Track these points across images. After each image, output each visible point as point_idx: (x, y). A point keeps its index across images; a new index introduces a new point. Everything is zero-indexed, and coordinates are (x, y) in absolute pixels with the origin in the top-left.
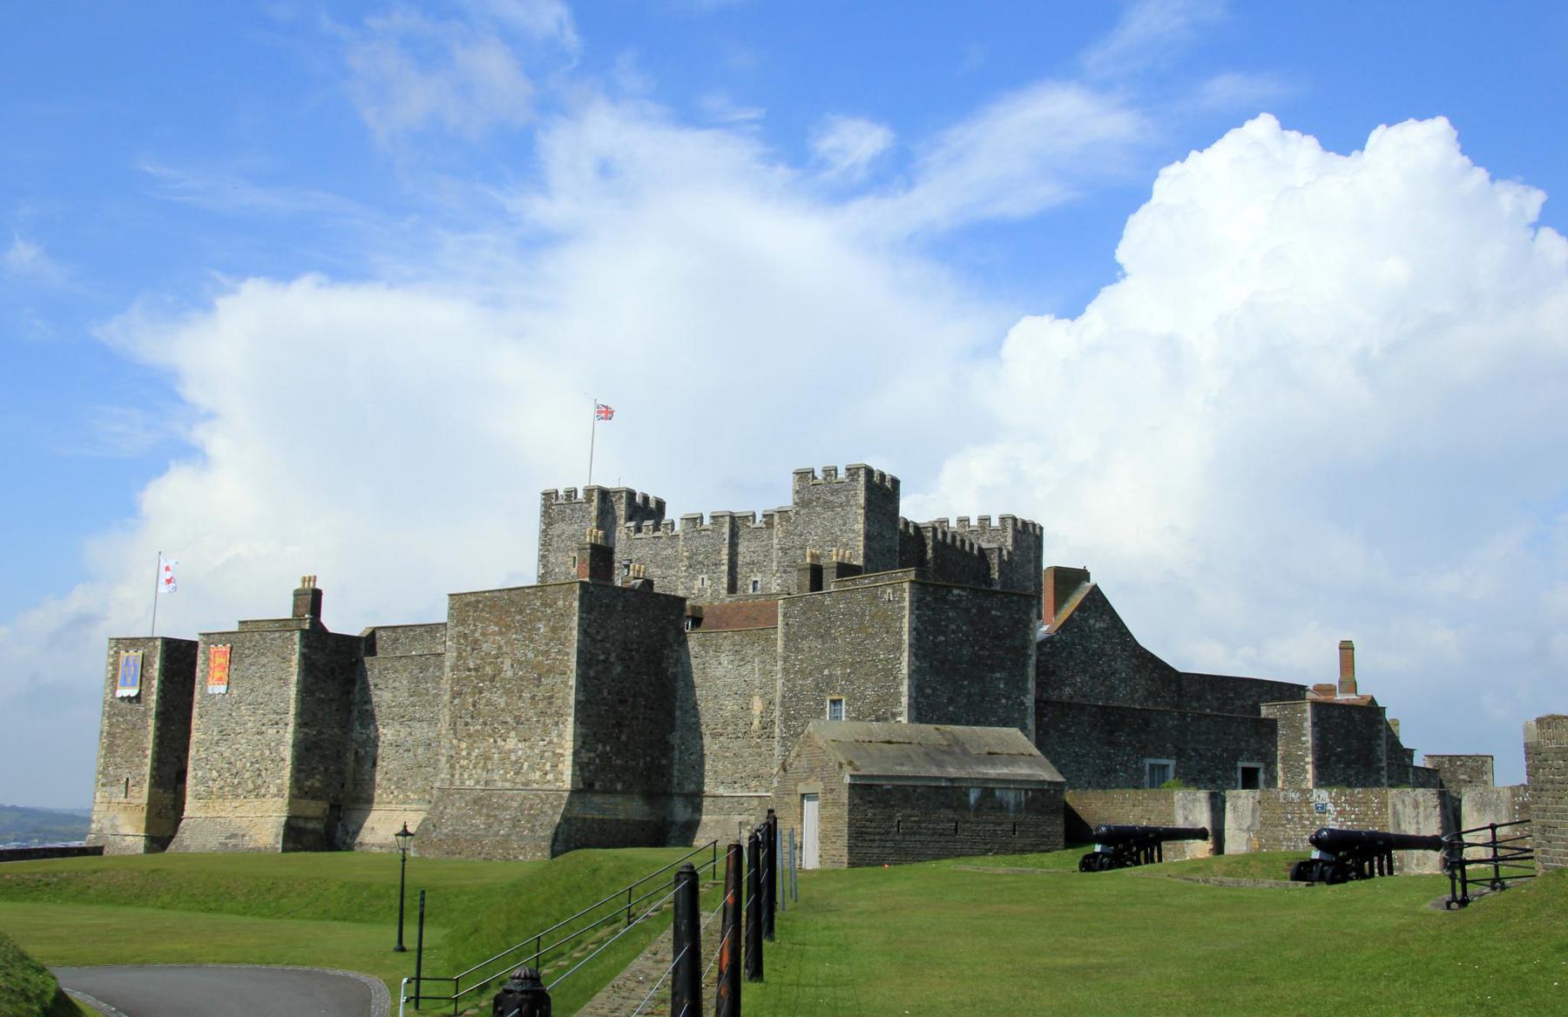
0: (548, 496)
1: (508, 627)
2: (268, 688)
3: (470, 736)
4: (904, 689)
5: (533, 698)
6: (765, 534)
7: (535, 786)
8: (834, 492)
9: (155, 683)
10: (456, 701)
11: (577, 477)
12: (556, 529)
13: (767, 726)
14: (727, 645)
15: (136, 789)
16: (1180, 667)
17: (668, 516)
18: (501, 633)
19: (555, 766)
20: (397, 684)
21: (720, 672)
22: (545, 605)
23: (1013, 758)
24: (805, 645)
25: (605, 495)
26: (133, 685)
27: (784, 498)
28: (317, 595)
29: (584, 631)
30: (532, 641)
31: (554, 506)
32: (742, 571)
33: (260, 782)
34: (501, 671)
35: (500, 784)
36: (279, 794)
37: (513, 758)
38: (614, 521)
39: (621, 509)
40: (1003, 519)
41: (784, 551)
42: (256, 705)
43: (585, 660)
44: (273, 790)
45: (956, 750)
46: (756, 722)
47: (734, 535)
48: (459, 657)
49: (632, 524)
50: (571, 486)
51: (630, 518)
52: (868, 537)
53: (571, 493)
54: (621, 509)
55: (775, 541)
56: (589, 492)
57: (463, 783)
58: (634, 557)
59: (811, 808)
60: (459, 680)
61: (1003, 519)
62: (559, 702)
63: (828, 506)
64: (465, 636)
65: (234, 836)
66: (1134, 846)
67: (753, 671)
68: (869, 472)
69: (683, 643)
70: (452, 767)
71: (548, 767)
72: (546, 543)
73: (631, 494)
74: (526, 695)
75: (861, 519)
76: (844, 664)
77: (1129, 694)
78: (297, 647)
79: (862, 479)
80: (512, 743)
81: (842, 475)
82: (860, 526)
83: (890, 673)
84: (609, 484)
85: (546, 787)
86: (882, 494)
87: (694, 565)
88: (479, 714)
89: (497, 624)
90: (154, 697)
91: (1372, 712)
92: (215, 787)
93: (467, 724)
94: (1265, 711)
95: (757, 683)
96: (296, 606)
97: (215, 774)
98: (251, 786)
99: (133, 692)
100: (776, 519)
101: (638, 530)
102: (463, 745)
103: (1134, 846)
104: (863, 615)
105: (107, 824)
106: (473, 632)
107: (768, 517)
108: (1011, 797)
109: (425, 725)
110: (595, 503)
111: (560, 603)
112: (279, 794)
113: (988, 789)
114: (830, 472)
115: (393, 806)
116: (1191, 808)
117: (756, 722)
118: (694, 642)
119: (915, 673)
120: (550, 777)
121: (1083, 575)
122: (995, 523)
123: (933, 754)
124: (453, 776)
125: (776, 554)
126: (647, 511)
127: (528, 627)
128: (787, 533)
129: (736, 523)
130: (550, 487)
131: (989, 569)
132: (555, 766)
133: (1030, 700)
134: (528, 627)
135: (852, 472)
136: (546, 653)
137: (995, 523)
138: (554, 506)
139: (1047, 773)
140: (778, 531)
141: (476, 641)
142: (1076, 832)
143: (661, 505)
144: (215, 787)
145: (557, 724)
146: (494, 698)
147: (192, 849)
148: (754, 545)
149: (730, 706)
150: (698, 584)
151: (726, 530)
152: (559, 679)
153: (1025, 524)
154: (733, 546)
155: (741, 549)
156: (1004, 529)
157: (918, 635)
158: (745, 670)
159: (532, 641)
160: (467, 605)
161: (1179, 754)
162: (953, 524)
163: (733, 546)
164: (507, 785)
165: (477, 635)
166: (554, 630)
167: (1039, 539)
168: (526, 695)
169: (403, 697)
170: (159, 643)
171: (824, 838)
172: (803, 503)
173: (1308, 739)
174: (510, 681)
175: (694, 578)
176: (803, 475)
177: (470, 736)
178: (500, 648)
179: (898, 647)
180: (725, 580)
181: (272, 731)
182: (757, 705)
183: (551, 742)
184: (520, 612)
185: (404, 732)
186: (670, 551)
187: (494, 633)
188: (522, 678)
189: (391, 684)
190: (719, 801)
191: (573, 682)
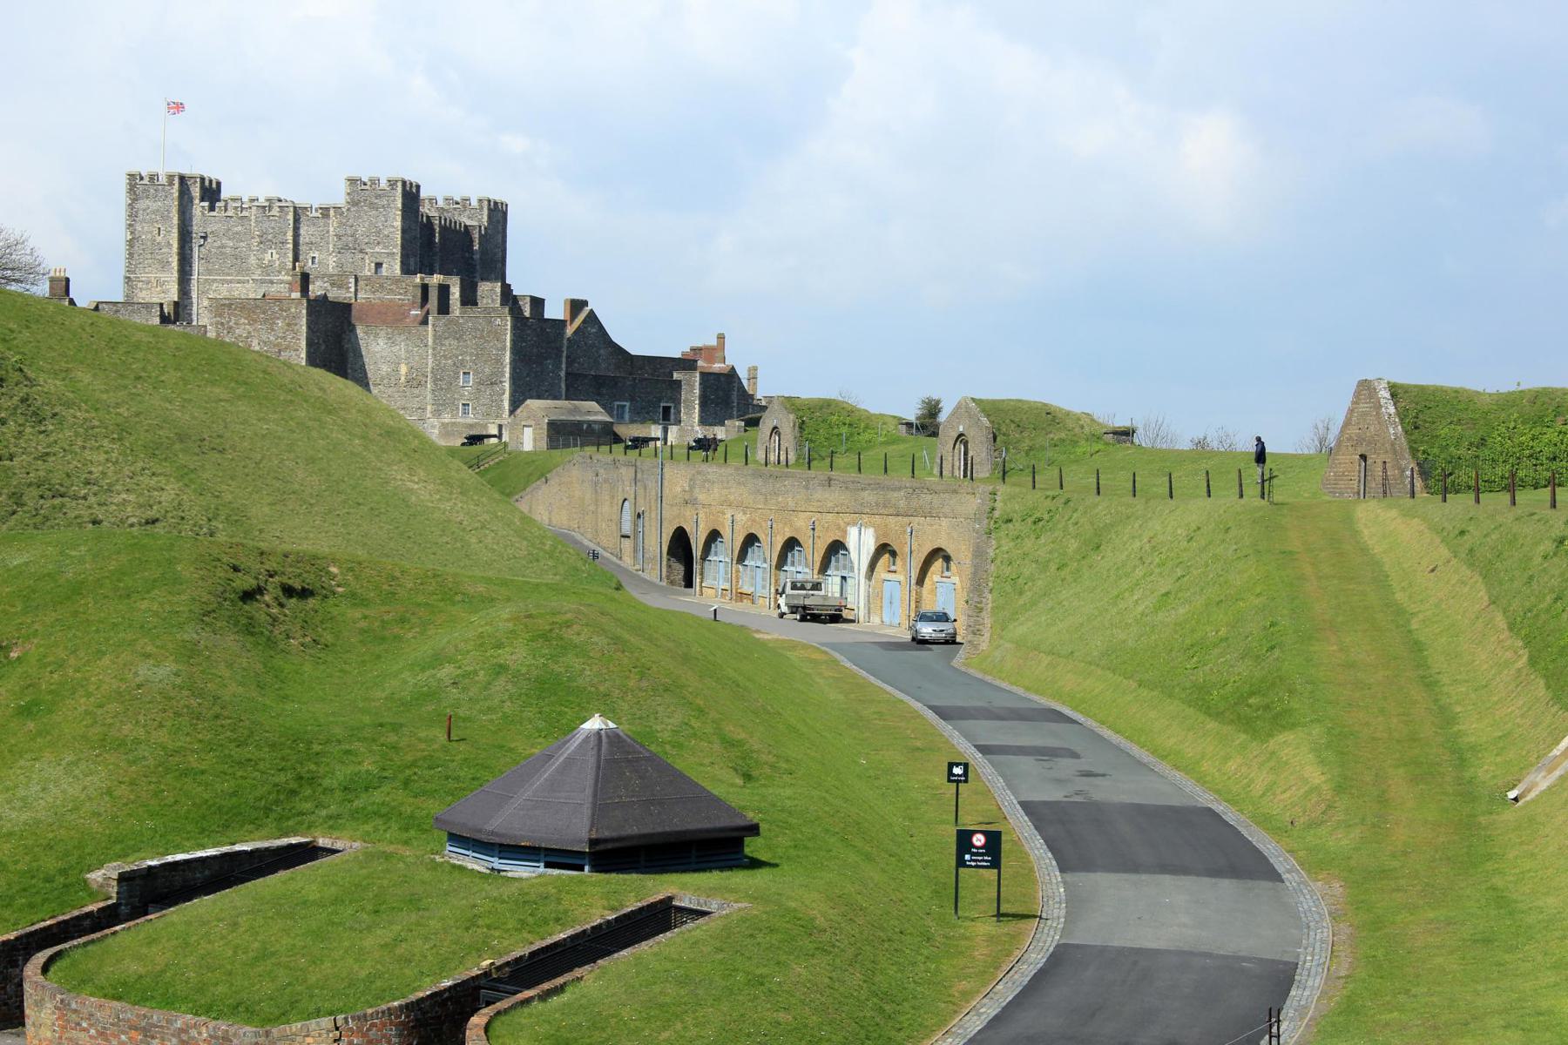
0: (132, 176)
1: (255, 321)
4: (507, 369)
6: (322, 222)
8: (378, 197)
11: (165, 166)
12: (141, 204)
13: (414, 382)
14: (382, 334)
16: (634, 350)
17: (225, 194)
21: (378, 349)
23: (596, 413)
25: (182, 178)
27: (338, 195)
28: (67, 280)
29: (309, 327)
31: (137, 185)
32: (302, 248)
38: (191, 200)
39: (196, 191)
40: (480, 201)
41: (339, 237)
43: (309, 344)
45: (576, 410)
47: (297, 221)
49: (206, 204)
50: (153, 170)
51: (202, 200)
52: (404, 231)
53: (152, 177)
54: (196, 191)
56: (171, 177)
59: (528, 432)
61: (480, 201)
63: (373, 206)
66: (639, 443)
67: (401, 349)
68: (404, 183)
69: (352, 329)
72: (133, 215)
73: (203, 179)
75: (399, 218)
77: (605, 368)
79: (399, 189)
81: (384, 184)
82: (398, 223)
83: (499, 361)
84: (186, 171)
86: (411, 196)
87: (264, 242)
91: (732, 375)
94: (676, 376)
101: (212, 208)
103: (639, 443)
107: (325, 212)
108: (596, 427)
110: (176, 186)
113: (589, 423)
114: (374, 182)
116: (656, 431)
118: (360, 331)
119: (513, 362)
121: (585, 303)
122: (474, 203)
123: (571, 412)
125: (333, 239)
126: (211, 193)
127: (270, 323)
128: (341, 224)
129: (298, 213)
130: (134, 170)
131: (471, 241)
133: (563, 374)
134: (270, 323)
135: (392, 183)
137: (474, 203)
138: (137, 185)
139: (608, 419)
140: (333, 223)
142: (617, 439)
143: (219, 184)
148: (312, 230)
149: (385, 368)
151: (290, 217)
153: (496, 203)
154: (296, 229)
155: (302, 232)
156: (481, 208)
157: (514, 342)
158: (396, 349)
161: (632, 399)
162: (441, 203)
163: (296, 229)
167: (505, 214)
171: (535, 440)
172: (354, 203)
173: (697, 391)
175: (265, 251)
176: (353, 181)
179: (504, 348)
180: (290, 255)
182: (403, 369)
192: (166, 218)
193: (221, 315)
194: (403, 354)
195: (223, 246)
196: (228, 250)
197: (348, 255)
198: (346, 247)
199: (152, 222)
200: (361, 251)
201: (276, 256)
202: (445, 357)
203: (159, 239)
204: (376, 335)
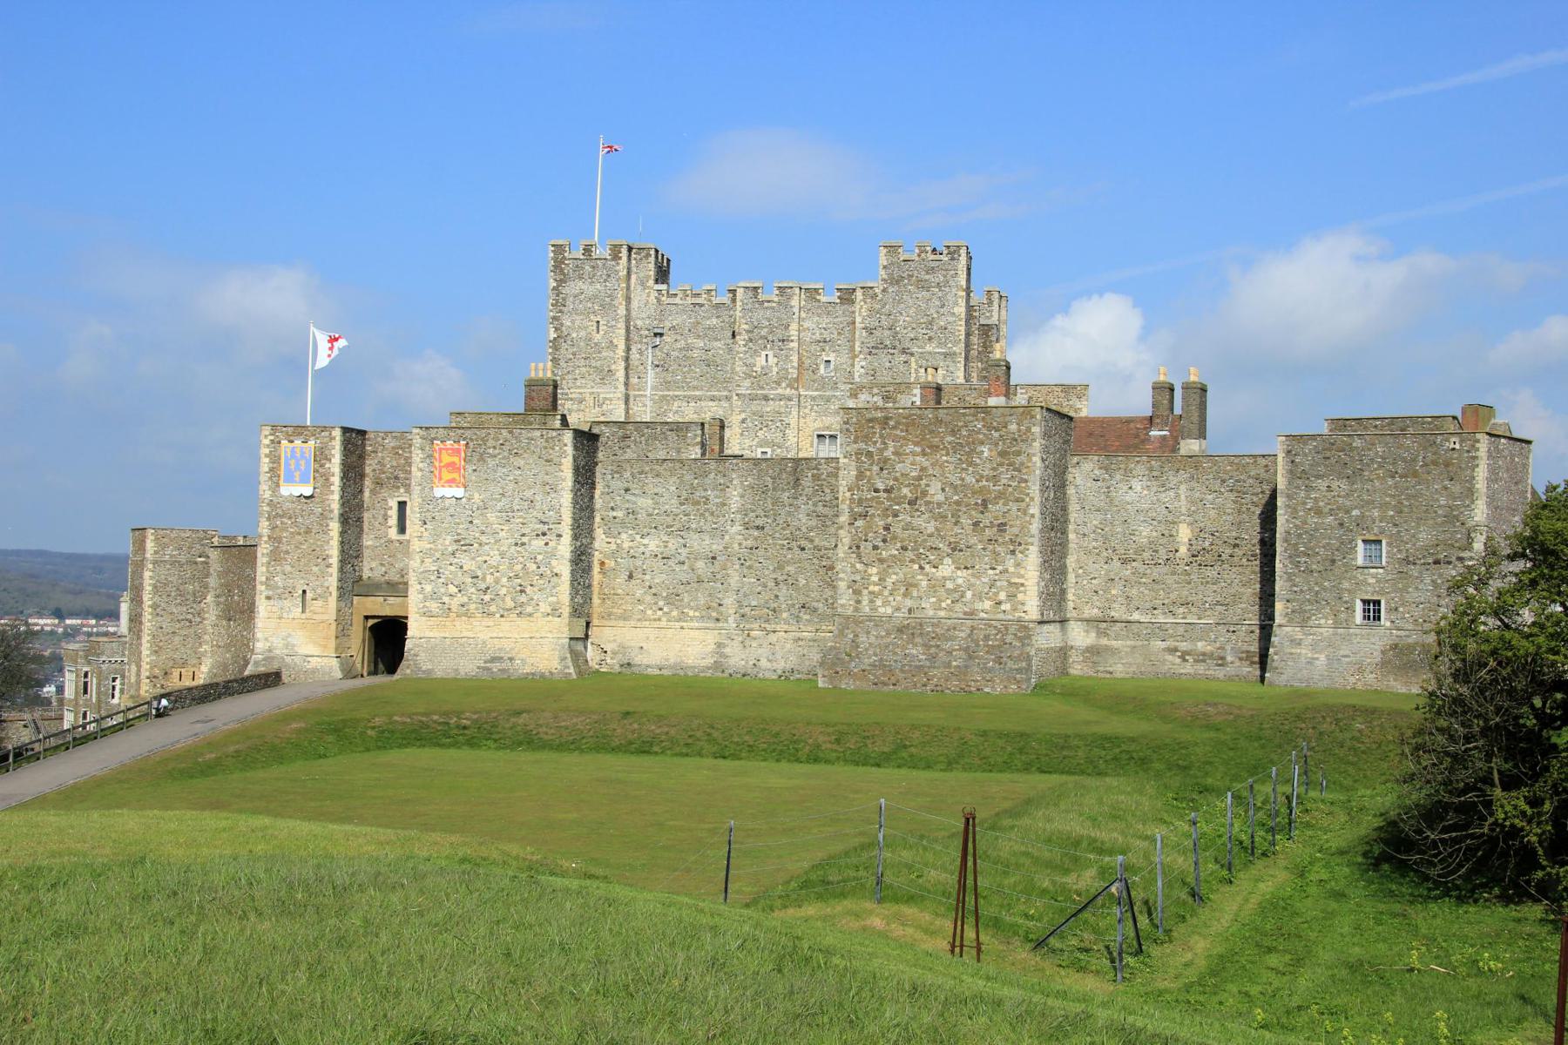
1: (934, 448)
2: (528, 494)
3: (881, 561)
5: (976, 524)
6: (840, 310)
7: (983, 615)
9: (336, 480)
10: (859, 523)
12: (572, 288)
15: (319, 603)
18: (924, 454)
19: (1012, 596)
20: (659, 490)
22: (990, 428)
24: (1322, 484)
26: (304, 481)
30: (971, 464)
33: (523, 598)
34: (924, 493)
35: (931, 613)
36: (555, 611)
37: (950, 585)
42: (508, 515)
44: (545, 608)
46: (1183, 550)
48: (860, 476)
55: (858, 319)
57: (874, 609)
58: (668, 324)
60: (860, 501)
62: (1015, 530)
63: (923, 285)
64: (869, 454)
65: (493, 660)
70: (857, 592)
71: (1002, 596)
74: (966, 521)
76: (1384, 506)
78: (570, 450)
80: (947, 568)
85: (1001, 616)
88: (894, 538)
89: (916, 444)
90: (336, 497)
92: (454, 604)
93: (875, 548)
95: (1184, 510)
96: (529, 398)
97: (453, 589)
98: (510, 604)
99: (308, 491)
100: (859, 294)
102: (875, 570)
104: (1414, 460)
105: (278, 644)
106: (881, 451)
109: (706, 537)
111: (1013, 427)
112: (555, 611)
115: (663, 623)
117: (1183, 550)
120: (1006, 607)
124: (858, 602)
125: (860, 334)
127: (966, 451)
132: (1012, 596)
134: (966, 451)
136: (995, 479)
141: (886, 460)
144: (454, 604)
145: (1013, 552)
146: (919, 522)
147: (439, 674)
148: (825, 321)
150: (761, 361)
152: (1014, 507)
158: (1167, 497)
159: (971, 464)
160: (870, 420)
164: (942, 614)
165: (888, 453)
166: (1003, 454)
168: (965, 521)
169: (672, 504)
170: (337, 433)
172: (895, 281)
174: (939, 505)
177: (881, 561)
178: (923, 469)
181: (540, 542)
182: (1184, 533)
183: (1006, 571)
184: (953, 433)
185: (673, 544)
186: (714, 321)
187: (913, 453)
188: (958, 503)
189: (651, 489)
190: (1134, 627)
191: (1035, 510)
192: (607, 307)
193: (867, 439)
194: (1183, 504)
195: (689, 348)
197: (884, 358)
198: (880, 346)
199: (588, 313)
200: (904, 351)
202: (1319, 512)
203: (597, 337)
204: (1128, 473)
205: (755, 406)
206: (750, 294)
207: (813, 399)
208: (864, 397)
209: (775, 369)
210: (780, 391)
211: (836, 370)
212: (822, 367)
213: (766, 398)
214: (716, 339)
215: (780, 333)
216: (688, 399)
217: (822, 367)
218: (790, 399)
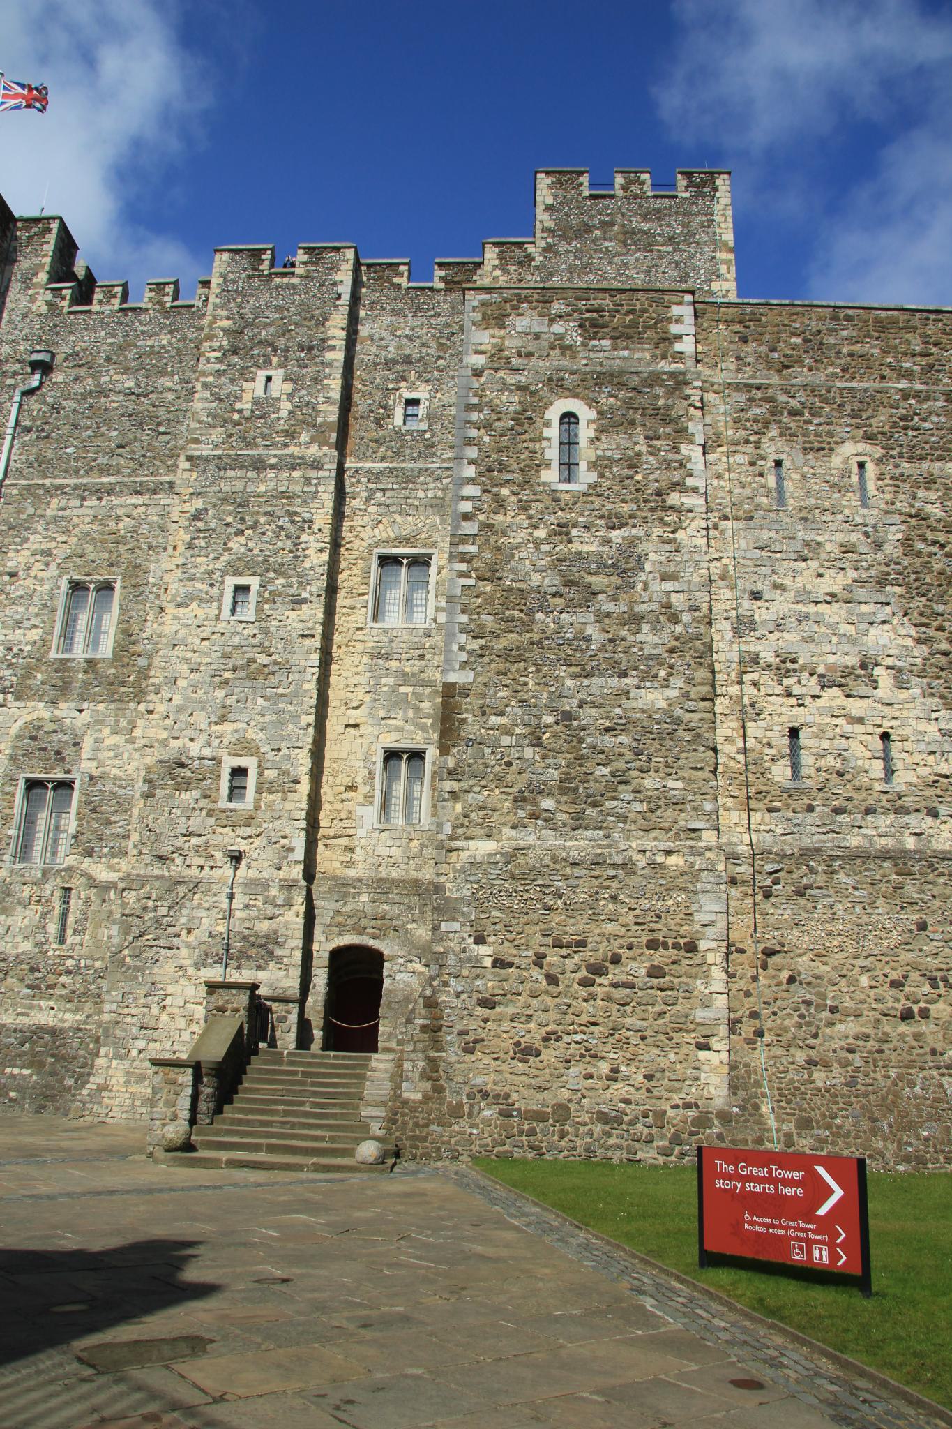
148: (408, 324)
150: (256, 388)
186: (164, 339)
196: (115, 402)
201: (280, 387)
205: (232, 482)
206: (245, 263)
207: (374, 476)
208: (525, 322)
209: (286, 406)
210: (293, 450)
211: (432, 417)
212: (398, 413)
213: (259, 465)
214: (163, 373)
215: (302, 335)
216: (82, 493)
217: (398, 413)
218: (316, 465)
